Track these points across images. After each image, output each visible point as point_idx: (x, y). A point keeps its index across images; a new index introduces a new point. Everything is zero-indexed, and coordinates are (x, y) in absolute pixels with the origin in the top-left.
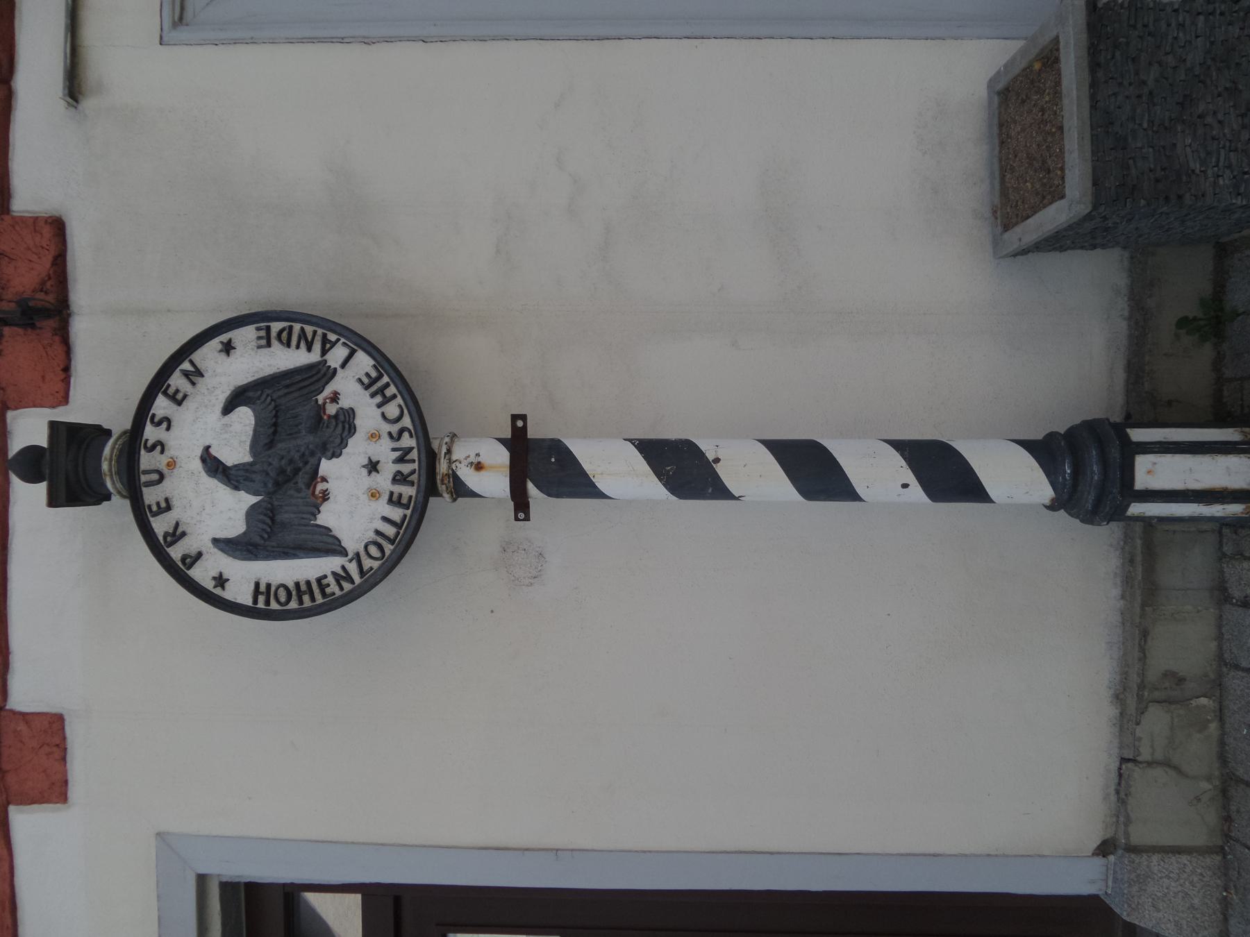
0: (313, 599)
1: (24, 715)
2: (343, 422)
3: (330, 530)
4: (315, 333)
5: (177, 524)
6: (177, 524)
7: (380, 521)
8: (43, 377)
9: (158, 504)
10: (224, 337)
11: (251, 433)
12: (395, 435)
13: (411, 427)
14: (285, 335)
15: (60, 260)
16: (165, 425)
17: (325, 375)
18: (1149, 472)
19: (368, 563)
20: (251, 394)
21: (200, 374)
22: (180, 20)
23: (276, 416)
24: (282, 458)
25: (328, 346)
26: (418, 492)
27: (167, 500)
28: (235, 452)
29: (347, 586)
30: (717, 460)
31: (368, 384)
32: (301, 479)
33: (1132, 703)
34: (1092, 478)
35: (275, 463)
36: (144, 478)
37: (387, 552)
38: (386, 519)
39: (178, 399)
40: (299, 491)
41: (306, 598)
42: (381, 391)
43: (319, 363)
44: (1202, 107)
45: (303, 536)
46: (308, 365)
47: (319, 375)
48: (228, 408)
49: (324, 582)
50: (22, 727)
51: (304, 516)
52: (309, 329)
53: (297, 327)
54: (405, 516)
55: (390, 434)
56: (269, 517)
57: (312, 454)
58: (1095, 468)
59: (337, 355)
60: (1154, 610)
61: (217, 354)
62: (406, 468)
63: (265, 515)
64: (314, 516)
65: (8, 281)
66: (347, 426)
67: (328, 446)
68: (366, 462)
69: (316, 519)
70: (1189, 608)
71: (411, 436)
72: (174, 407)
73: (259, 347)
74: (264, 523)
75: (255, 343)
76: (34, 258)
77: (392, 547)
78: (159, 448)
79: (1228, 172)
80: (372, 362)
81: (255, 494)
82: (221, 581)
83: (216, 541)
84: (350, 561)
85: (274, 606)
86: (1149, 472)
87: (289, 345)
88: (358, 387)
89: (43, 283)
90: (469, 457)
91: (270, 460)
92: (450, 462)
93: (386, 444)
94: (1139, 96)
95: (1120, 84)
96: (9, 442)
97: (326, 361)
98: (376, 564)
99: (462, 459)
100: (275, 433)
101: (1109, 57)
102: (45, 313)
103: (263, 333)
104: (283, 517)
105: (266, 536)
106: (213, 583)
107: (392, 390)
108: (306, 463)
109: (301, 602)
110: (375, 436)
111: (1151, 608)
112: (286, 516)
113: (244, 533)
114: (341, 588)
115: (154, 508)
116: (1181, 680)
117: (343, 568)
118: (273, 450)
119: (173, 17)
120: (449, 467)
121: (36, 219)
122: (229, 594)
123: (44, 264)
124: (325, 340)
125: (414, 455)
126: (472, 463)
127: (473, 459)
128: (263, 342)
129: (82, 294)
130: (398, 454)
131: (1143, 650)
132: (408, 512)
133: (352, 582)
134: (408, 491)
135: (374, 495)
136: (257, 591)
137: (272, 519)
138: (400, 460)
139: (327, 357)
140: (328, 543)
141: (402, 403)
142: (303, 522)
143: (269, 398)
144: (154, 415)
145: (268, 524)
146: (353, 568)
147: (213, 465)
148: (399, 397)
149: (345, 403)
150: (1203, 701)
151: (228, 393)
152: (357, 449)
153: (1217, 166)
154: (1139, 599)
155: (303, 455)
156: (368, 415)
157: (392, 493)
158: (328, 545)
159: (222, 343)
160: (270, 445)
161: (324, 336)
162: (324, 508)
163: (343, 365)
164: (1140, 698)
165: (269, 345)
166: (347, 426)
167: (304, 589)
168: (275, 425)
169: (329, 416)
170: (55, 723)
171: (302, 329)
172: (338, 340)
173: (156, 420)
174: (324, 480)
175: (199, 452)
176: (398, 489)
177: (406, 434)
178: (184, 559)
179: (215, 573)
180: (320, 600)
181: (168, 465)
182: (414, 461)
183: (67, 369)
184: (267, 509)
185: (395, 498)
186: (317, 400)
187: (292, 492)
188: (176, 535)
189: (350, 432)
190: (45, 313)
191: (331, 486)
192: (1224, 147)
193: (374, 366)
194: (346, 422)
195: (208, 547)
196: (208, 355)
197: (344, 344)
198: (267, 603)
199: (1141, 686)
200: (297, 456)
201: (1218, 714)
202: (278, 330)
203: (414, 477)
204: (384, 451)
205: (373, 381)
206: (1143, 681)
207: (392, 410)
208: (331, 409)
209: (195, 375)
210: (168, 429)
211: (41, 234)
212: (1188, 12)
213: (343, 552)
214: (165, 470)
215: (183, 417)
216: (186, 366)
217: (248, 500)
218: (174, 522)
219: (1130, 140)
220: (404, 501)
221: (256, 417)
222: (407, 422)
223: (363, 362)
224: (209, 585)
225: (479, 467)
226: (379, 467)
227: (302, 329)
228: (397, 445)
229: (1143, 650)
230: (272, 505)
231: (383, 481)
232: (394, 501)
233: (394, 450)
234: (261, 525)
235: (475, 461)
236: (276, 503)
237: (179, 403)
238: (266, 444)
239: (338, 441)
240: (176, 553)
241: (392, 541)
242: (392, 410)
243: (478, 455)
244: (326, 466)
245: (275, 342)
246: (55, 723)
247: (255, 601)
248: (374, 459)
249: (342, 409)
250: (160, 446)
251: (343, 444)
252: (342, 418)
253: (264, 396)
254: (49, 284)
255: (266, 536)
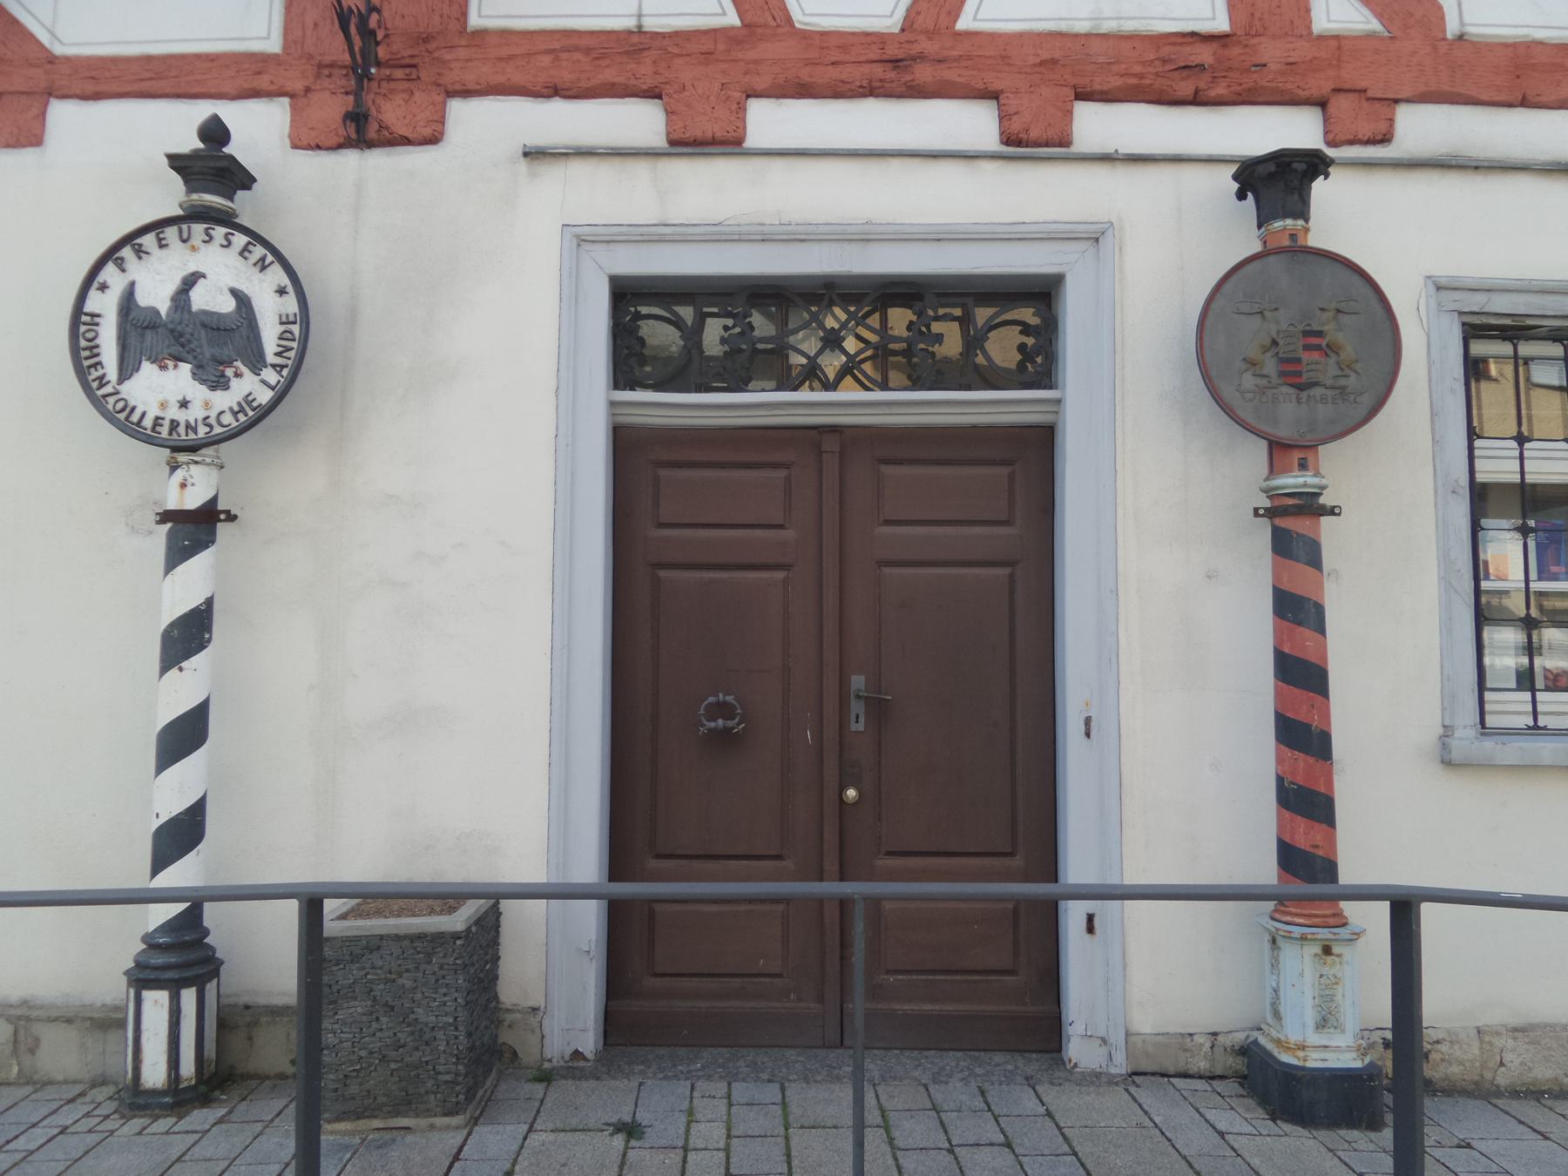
0: (87, 358)
1: (43, 114)
2: (218, 382)
3: (138, 370)
4: (289, 359)
5: (147, 253)
6: (147, 253)
7: (143, 410)
8: (312, 129)
9: (164, 239)
10: (290, 289)
11: (214, 310)
12: (207, 421)
13: (213, 433)
14: (289, 335)
15: (406, 141)
16: (225, 243)
17: (255, 367)
18: (156, 1001)
19: (111, 400)
20: (244, 310)
21: (263, 268)
22: (581, 241)
23: (225, 330)
24: (192, 335)
25: (278, 369)
26: (163, 438)
27: (167, 245)
28: (200, 299)
29: (95, 385)
30: (181, 669)
31: (248, 399)
32: (176, 349)
33: (19, 1012)
34: (153, 959)
35: (188, 330)
36: (185, 227)
37: (118, 416)
38: (143, 415)
39: (244, 253)
40: (168, 347)
41: (87, 353)
42: (242, 410)
43: (265, 361)
44: (384, 1020)
45: (133, 350)
46: (264, 354)
47: (256, 362)
48: (235, 293)
49: (99, 367)
50: (34, 111)
51: (148, 352)
52: (292, 354)
53: (294, 345)
54: (146, 429)
55: (207, 417)
56: (148, 325)
57: (195, 358)
58: (160, 960)
59: (271, 376)
60: (87, 1029)
61: (277, 283)
62: (182, 429)
63: (150, 322)
64: (148, 360)
65: (390, 100)
66: (214, 384)
67: (200, 370)
68: (188, 399)
69: (146, 360)
70: (89, 1058)
71: (206, 433)
72: (239, 249)
73: (280, 316)
74: (144, 321)
75: (284, 312)
76: (406, 121)
77: (122, 419)
78: (207, 238)
79: (337, 1041)
80: (264, 403)
81: (168, 315)
82: (103, 287)
83: (132, 284)
84: (114, 387)
85: (83, 328)
86: (156, 1001)
87: (280, 339)
88: (246, 393)
89: (387, 128)
90: (192, 477)
91: (191, 326)
92: (188, 464)
93: (201, 414)
94: (390, 973)
95: (398, 958)
96: (264, 99)
97: (266, 367)
98: (110, 407)
99: (191, 473)
100: (212, 328)
101: (418, 949)
102: (360, 130)
103: (291, 318)
104: (149, 334)
105: (134, 322)
106: (101, 281)
107: (242, 418)
108: (188, 352)
109: (85, 349)
110: (207, 405)
111: (88, 1026)
112: (149, 338)
113: (137, 306)
114: (94, 380)
115: (161, 236)
116: (32, 1051)
117: (109, 382)
118: (199, 327)
119: (583, 235)
120: (184, 463)
121: (443, 123)
122: (93, 294)
123: (401, 130)
124: (283, 367)
125: (192, 436)
126: (186, 480)
127: (190, 480)
128: (284, 319)
129: (377, 161)
130: (193, 424)
131: (56, 1019)
132: (149, 432)
133: (99, 389)
134: (164, 431)
135: (163, 405)
136: (93, 315)
137: (147, 327)
138: (188, 426)
139: (270, 369)
140: (127, 370)
141: (232, 426)
142: (144, 352)
143: (239, 324)
144: (233, 234)
145: (142, 324)
146: (108, 389)
147: (190, 281)
148: (237, 424)
149: (234, 382)
150: (15, 1070)
151: (246, 292)
152: (198, 392)
153: (342, 1032)
154: (96, 1016)
155: (194, 351)
156: (224, 401)
157: (163, 419)
158: (127, 369)
159: (285, 287)
160: (204, 325)
161: (286, 366)
162: (155, 367)
163: (263, 382)
164: (19, 1018)
165: (282, 323)
166: (214, 384)
167: (94, 350)
168: (219, 329)
169: (223, 371)
170: (34, 138)
171: (293, 349)
172: (283, 377)
173: (230, 236)
174: (176, 367)
175: (202, 270)
176: (166, 423)
177: (208, 429)
178: (122, 259)
179: (110, 282)
180: (86, 363)
181: (193, 247)
182: (187, 435)
183: (318, 147)
184: (155, 323)
185: (160, 421)
186: (237, 360)
187: (167, 342)
188: (140, 252)
189: (213, 387)
190: (360, 130)
191: (171, 373)
192: (354, 1037)
193: (261, 405)
194: (220, 383)
195: (129, 277)
196: (277, 275)
197: (279, 381)
198: (85, 324)
199: (28, 1019)
200: (192, 346)
201: (6, 1081)
202: (294, 330)
203: (175, 436)
204: (195, 413)
205: (249, 403)
206: (31, 1020)
207: (227, 419)
208: (229, 372)
209: (262, 265)
210: (222, 246)
211: (425, 127)
212: (456, 1009)
213: (121, 381)
214: (189, 244)
215: (231, 257)
216: (270, 258)
217: (164, 307)
218: (149, 251)
219: (357, 965)
220: (158, 429)
221: (226, 314)
222: (218, 430)
223: (264, 397)
224: (101, 278)
225: (183, 486)
226: (183, 409)
227: (293, 349)
228: (199, 422)
229: (56, 1019)
230: (158, 327)
231: (174, 413)
232: (158, 421)
233: (196, 420)
234: (142, 318)
235: (188, 483)
236: (160, 330)
237: (241, 254)
238: (203, 322)
239: (205, 378)
240: (126, 252)
241: (127, 418)
242: (227, 419)
243: (193, 484)
244: (186, 368)
245: (284, 328)
246: (34, 138)
247: (86, 314)
248: (189, 405)
249: (229, 380)
250: (209, 239)
251: (203, 381)
252: (222, 380)
253: (242, 320)
254: (386, 133)
255: (134, 322)
